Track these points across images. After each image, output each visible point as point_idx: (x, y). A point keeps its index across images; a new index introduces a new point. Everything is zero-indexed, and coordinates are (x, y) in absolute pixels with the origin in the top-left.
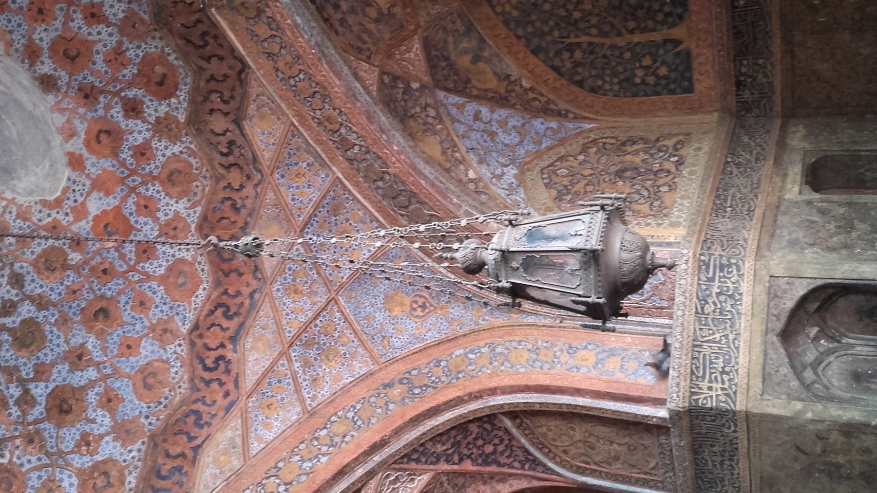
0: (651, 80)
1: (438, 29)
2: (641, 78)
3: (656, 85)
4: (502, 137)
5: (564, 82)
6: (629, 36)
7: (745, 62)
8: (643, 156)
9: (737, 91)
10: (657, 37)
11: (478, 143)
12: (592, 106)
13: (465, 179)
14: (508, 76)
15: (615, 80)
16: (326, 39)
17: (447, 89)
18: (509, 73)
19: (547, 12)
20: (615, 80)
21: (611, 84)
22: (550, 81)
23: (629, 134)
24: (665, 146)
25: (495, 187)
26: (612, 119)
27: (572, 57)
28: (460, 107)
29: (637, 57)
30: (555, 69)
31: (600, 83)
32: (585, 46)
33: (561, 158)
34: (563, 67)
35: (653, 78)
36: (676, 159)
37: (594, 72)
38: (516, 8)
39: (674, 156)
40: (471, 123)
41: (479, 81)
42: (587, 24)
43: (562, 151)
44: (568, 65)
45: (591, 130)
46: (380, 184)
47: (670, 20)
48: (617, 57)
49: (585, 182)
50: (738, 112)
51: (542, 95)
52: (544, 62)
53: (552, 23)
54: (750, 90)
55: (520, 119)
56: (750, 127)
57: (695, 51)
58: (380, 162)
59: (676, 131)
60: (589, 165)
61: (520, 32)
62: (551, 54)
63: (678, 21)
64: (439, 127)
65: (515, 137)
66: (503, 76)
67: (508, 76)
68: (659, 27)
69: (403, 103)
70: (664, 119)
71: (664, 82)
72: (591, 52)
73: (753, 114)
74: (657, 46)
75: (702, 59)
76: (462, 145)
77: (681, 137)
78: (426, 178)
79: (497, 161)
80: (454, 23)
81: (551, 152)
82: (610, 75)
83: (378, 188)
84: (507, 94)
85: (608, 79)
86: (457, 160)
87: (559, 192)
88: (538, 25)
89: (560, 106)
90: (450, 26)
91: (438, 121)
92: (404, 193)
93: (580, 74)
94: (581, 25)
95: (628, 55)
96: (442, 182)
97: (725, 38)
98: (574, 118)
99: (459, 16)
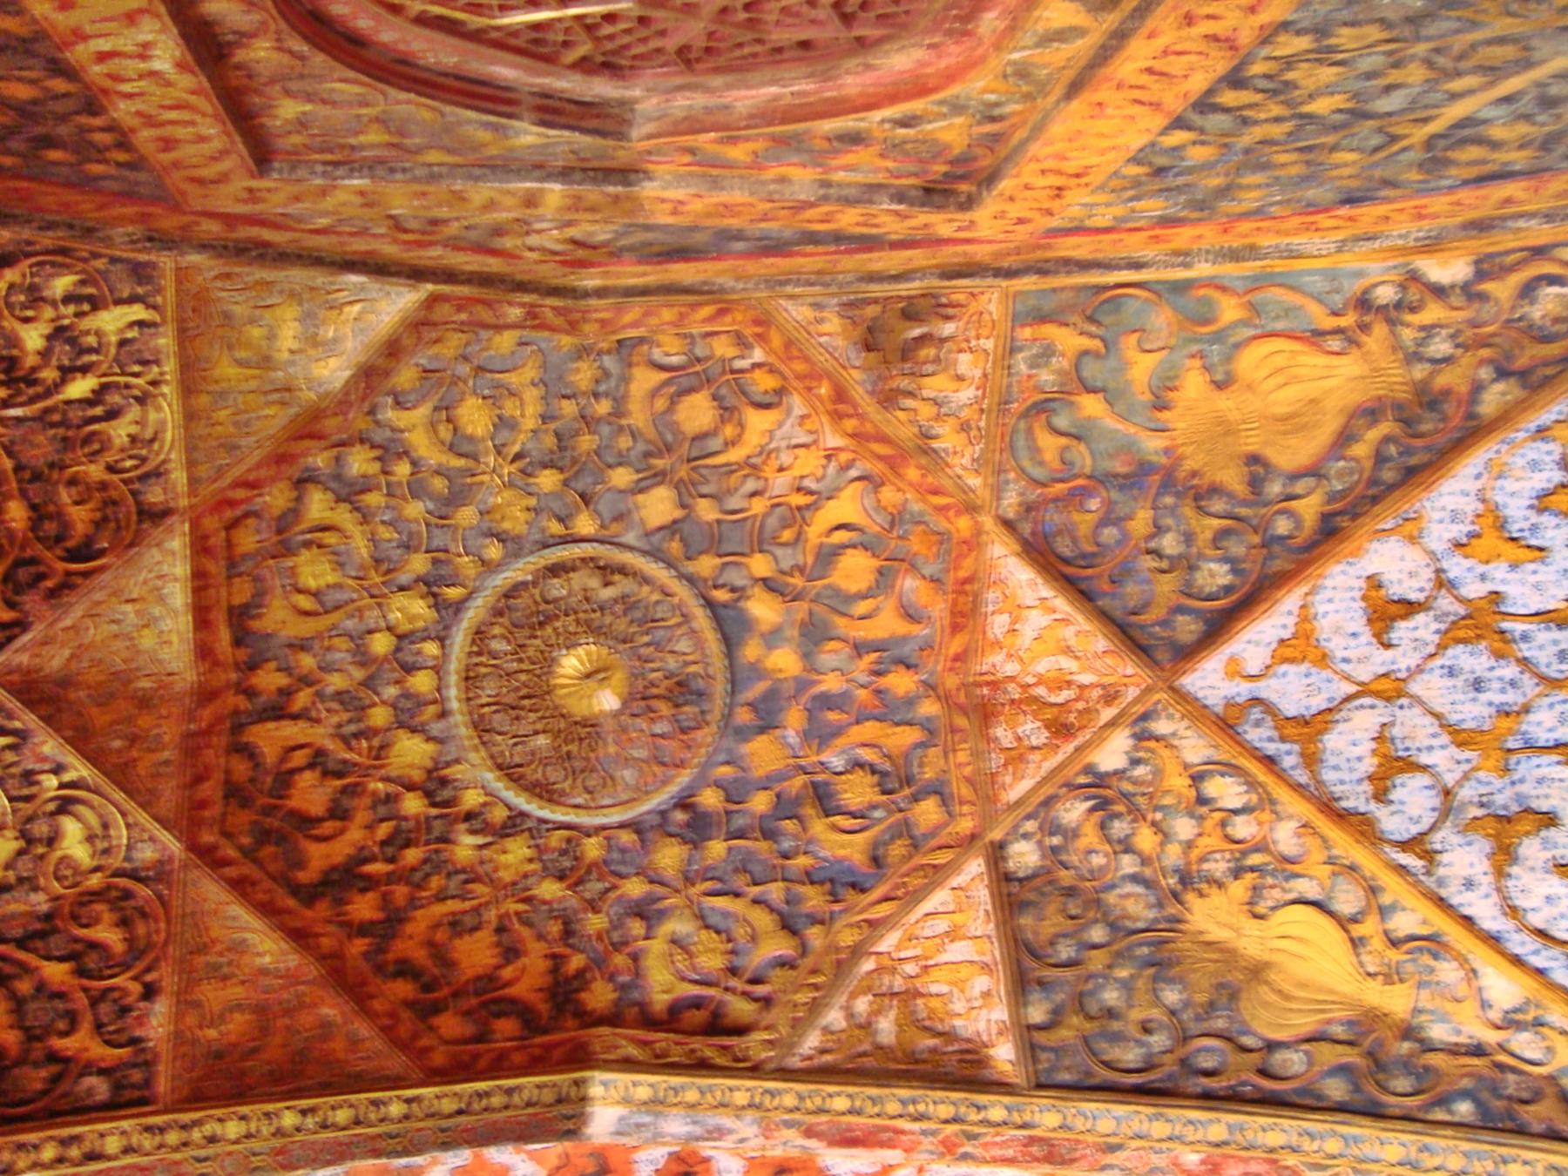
14: (1363, 303)
51: (1539, 252)
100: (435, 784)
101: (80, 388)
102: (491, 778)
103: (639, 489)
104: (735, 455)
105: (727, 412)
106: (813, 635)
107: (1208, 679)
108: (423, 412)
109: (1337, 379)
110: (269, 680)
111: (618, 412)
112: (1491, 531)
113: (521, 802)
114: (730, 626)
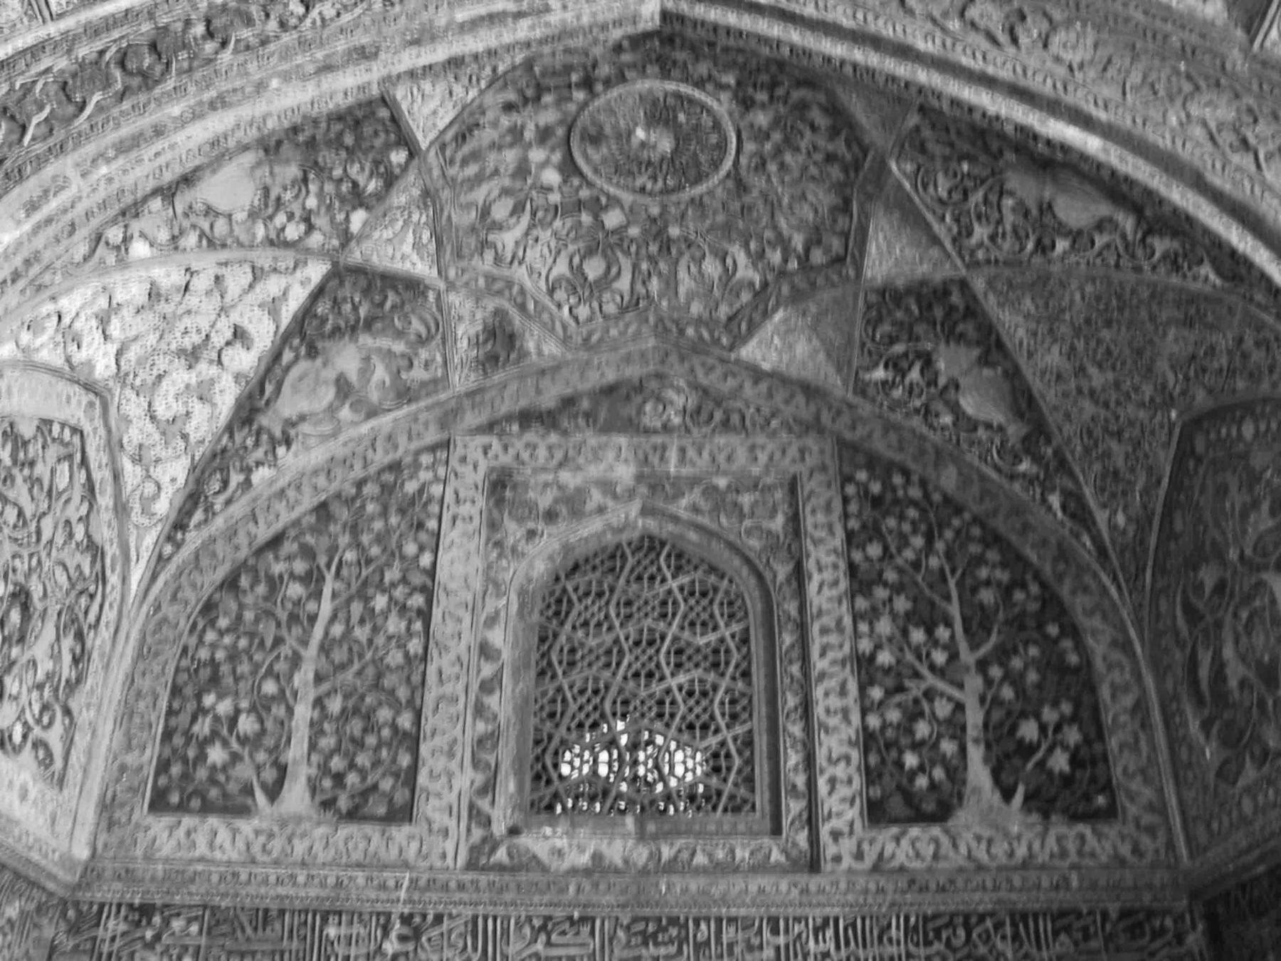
0: (203, 727)
1: (429, 330)
2: (213, 708)
3: (188, 736)
4: (180, 376)
5: (244, 553)
6: (312, 696)
7: (194, 928)
8: (45, 666)
9: (131, 906)
10: (296, 751)
11: (189, 312)
12: (174, 597)
13: (135, 226)
14: (288, 442)
15: (220, 655)
16: (548, 32)
17: (318, 293)
18: (294, 447)
19: (400, 547)
20: (220, 655)
21: (214, 646)
22: (251, 525)
23: (95, 655)
24: (50, 724)
25: (89, 292)
26: (135, 635)
27: (292, 576)
28: (273, 307)
29: (260, 707)
30: (275, 542)
31: (223, 622)
32: (311, 606)
33: (90, 487)
34: (277, 558)
35: (207, 730)
36: (17, 738)
37: (249, 616)
38: (421, 491)
39: (25, 737)
40: (235, 317)
41: (301, 379)
42: (355, 618)
43: (105, 500)
44: (278, 568)
45: (125, 580)
46: (199, 29)
47: (327, 783)
48: (271, 666)
49: (29, 510)
50: (77, 904)
51: (228, 502)
52: (296, 523)
53: (375, 551)
54: (124, 934)
55: (199, 436)
56: (36, 926)
57: (246, 827)
58: (254, 41)
59: (73, 758)
60: (60, 540)
61: (370, 489)
62: (309, 539)
63: (318, 799)
64: (260, 231)
65: (169, 407)
66: (292, 432)
67: (288, 442)
68: (315, 758)
69: (338, 172)
70: (106, 741)
71: (191, 753)
72: (294, 618)
73: (62, 937)
74: (275, 750)
75: (223, 836)
76: (207, 264)
77: (58, 764)
78: (182, 122)
79: (136, 339)
80: (427, 365)
81: (107, 474)
82: (235, 645)
83: (188, 23)
84: (255, 427)
85: (227, 640)
86: (182, 232)
87: (25, 444)
88: (378, 525)
89: (193, 534)
90: (424, 354)
91: (273, 235)
92: (158, 69)
93: (252, 587)
94: (357, 608)
95: (270, 687)
96: (157, 154)
97: (263, 890)
98: (160, 557)
99: (435, 381)
100: (747, 104)
101: (899, 348)
102: (715, 105)
103: (624, 228)
104: (571, 248)
105: (578, 271)
106: (522, 170)
107: (316, 271)
108: (739, 274)
109: (289, 405)
110: (835, 172)
111: (635, 267)
112: (204, 393)
113: (697, 94)
114: (569, 168)
